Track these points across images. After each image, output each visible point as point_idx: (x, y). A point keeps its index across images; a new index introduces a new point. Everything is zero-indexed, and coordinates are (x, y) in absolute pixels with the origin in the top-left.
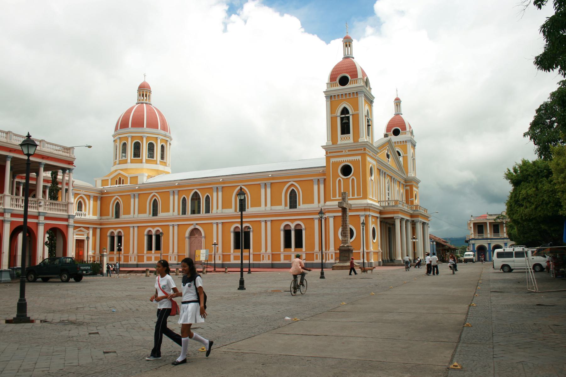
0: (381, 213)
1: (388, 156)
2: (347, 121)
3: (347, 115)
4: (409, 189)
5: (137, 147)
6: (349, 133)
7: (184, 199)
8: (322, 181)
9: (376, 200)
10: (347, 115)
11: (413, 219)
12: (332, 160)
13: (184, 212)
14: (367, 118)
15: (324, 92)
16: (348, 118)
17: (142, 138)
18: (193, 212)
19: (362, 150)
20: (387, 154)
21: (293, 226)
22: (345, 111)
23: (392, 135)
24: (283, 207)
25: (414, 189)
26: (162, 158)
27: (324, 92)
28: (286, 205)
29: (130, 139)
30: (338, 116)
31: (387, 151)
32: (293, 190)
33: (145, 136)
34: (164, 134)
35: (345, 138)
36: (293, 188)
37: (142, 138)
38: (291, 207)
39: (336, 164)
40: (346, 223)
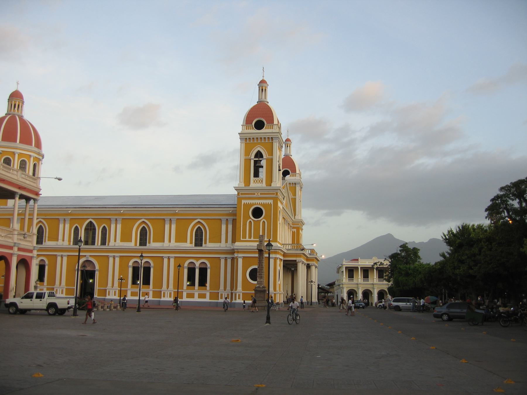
0: (285, 255)
7: (76, 229)
8: (230, 222)
11: (308, 263)
12: (243, 202)
15: (239, 134)
17: (14, 154)
19: (274, 194)
21: (197, 264)
22: (259, 155)
24: (189, 245)
27: (239, 134)
28: (191, 243)
30: (253, 159)
34: (38, 151)
35: (258, 181)
37: (14, 154)
39: (247, 206)
40: (262, 265)
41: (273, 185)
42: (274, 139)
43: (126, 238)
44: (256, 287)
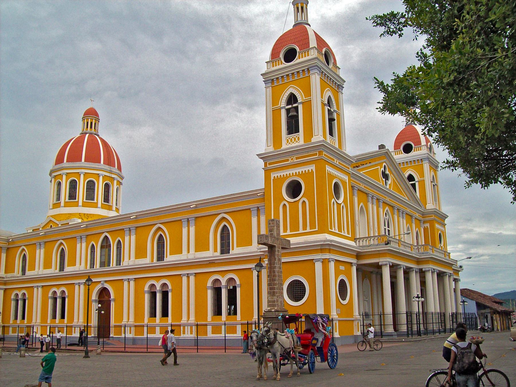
0: (359, 256)
1: (385, 176)
2: (295, 114)
3: (295, 105)
4: (429, 227)
5: (73, 187)
6: (297, 131)
10: (295, 105)
11: (421, 267)
12: (273, 175)
13: (92, 265)
14: (327, 108)
16: (296, 108)
17: (79, 174)
18: (102, 264)
19: (316, 154)
22: (292, 99)
23: (402, 152)
25: (437, 226)
26: (106, 199)
28: (216, 251)
29: (64, 177)
31: (383, 169)
32: (225, 226)
33: (83, 172)
34: (109, 169)
35: (293, 140)
36: (224, 223)
37: (79, 174)
39: (279, 181)
40: (274, 272)
41: (313, 140)
42: (311, 70)
43: (141, 252)
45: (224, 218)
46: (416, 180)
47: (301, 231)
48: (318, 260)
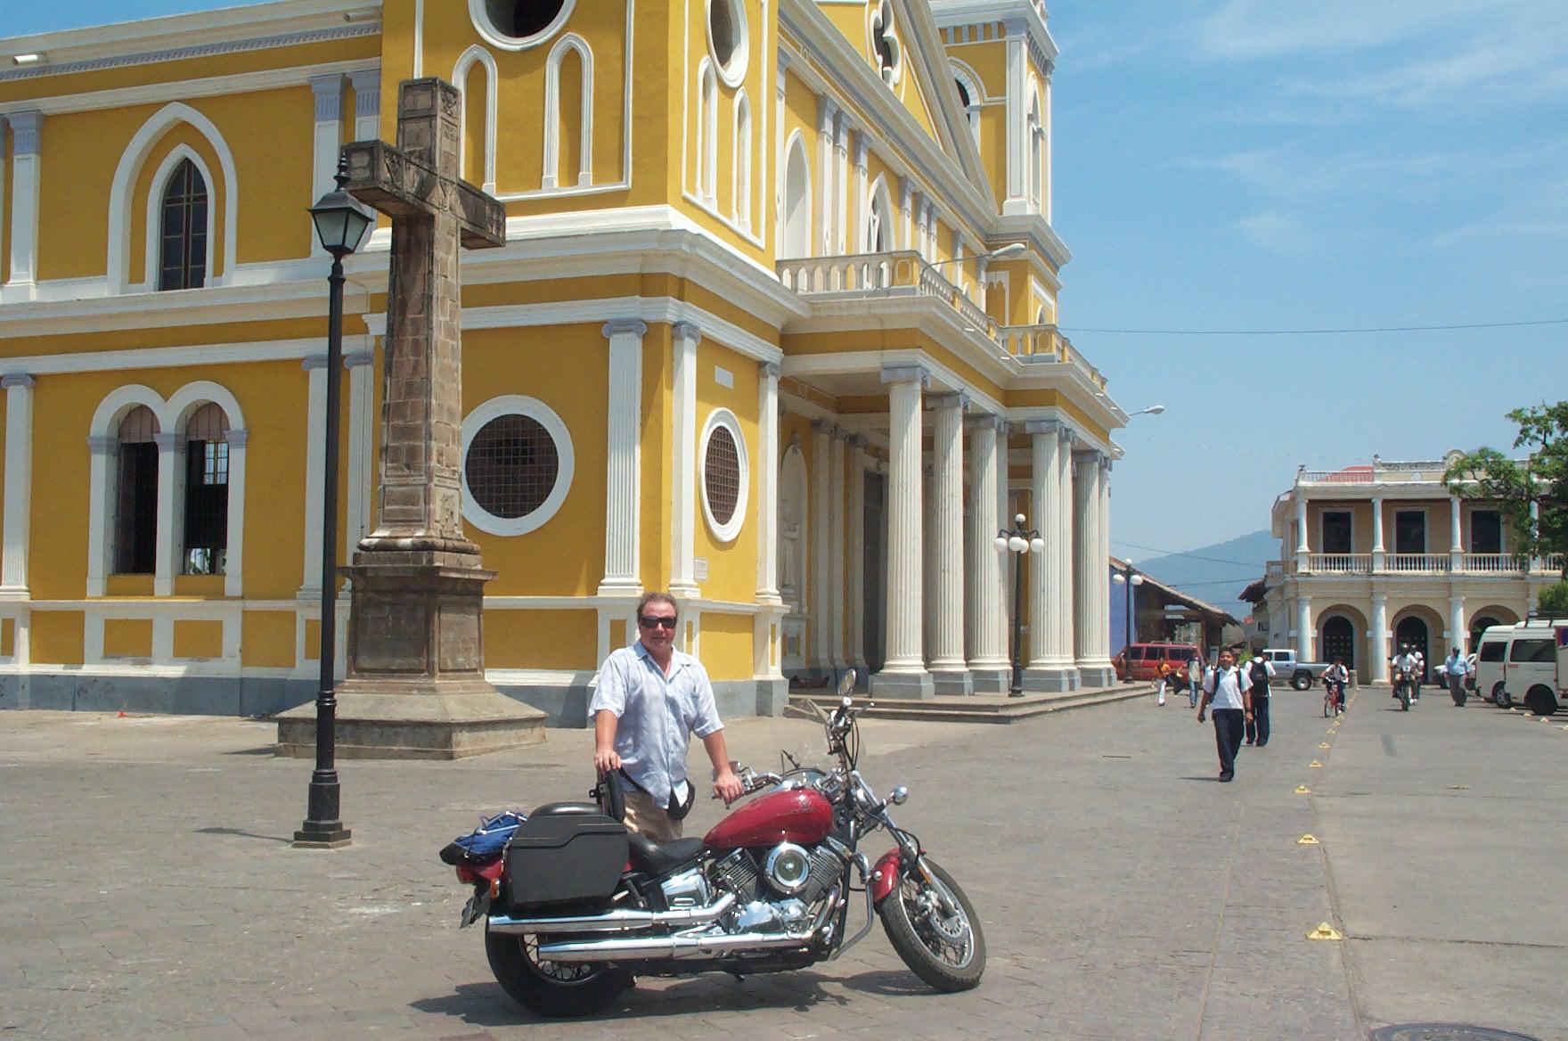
1: (885, 49)
4: (1006, 286)
9: (761, 243)
11: (1019, 414)
20: (879, 31)
21: (169, 415)
25: (1034, 285)
28: (136, 275)
38: (168, 281)
44: (362, 547)
45: (182, 131)
46: (972, 104)
47: (553, 185)
48: (624, 326)
